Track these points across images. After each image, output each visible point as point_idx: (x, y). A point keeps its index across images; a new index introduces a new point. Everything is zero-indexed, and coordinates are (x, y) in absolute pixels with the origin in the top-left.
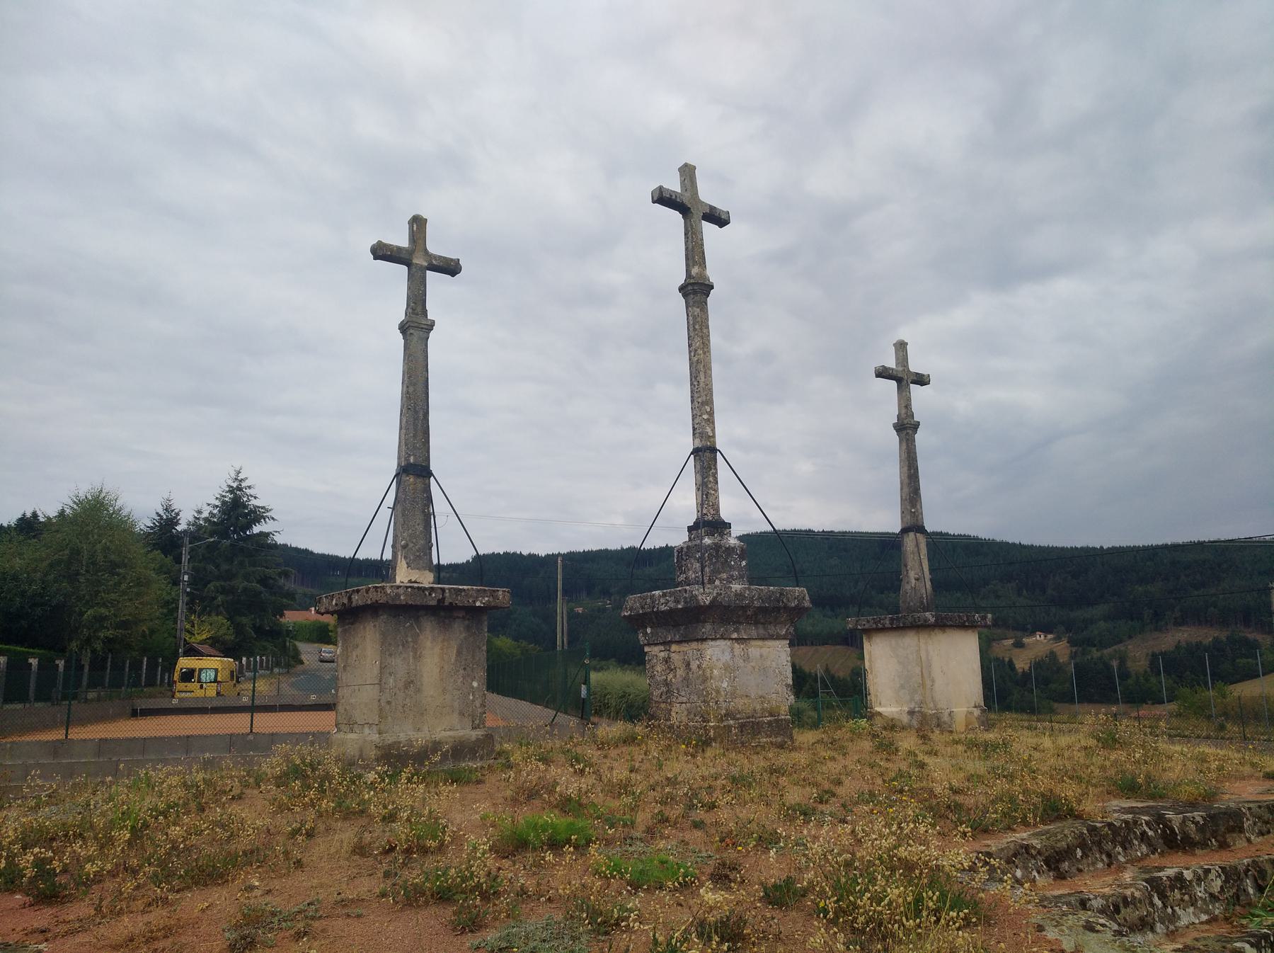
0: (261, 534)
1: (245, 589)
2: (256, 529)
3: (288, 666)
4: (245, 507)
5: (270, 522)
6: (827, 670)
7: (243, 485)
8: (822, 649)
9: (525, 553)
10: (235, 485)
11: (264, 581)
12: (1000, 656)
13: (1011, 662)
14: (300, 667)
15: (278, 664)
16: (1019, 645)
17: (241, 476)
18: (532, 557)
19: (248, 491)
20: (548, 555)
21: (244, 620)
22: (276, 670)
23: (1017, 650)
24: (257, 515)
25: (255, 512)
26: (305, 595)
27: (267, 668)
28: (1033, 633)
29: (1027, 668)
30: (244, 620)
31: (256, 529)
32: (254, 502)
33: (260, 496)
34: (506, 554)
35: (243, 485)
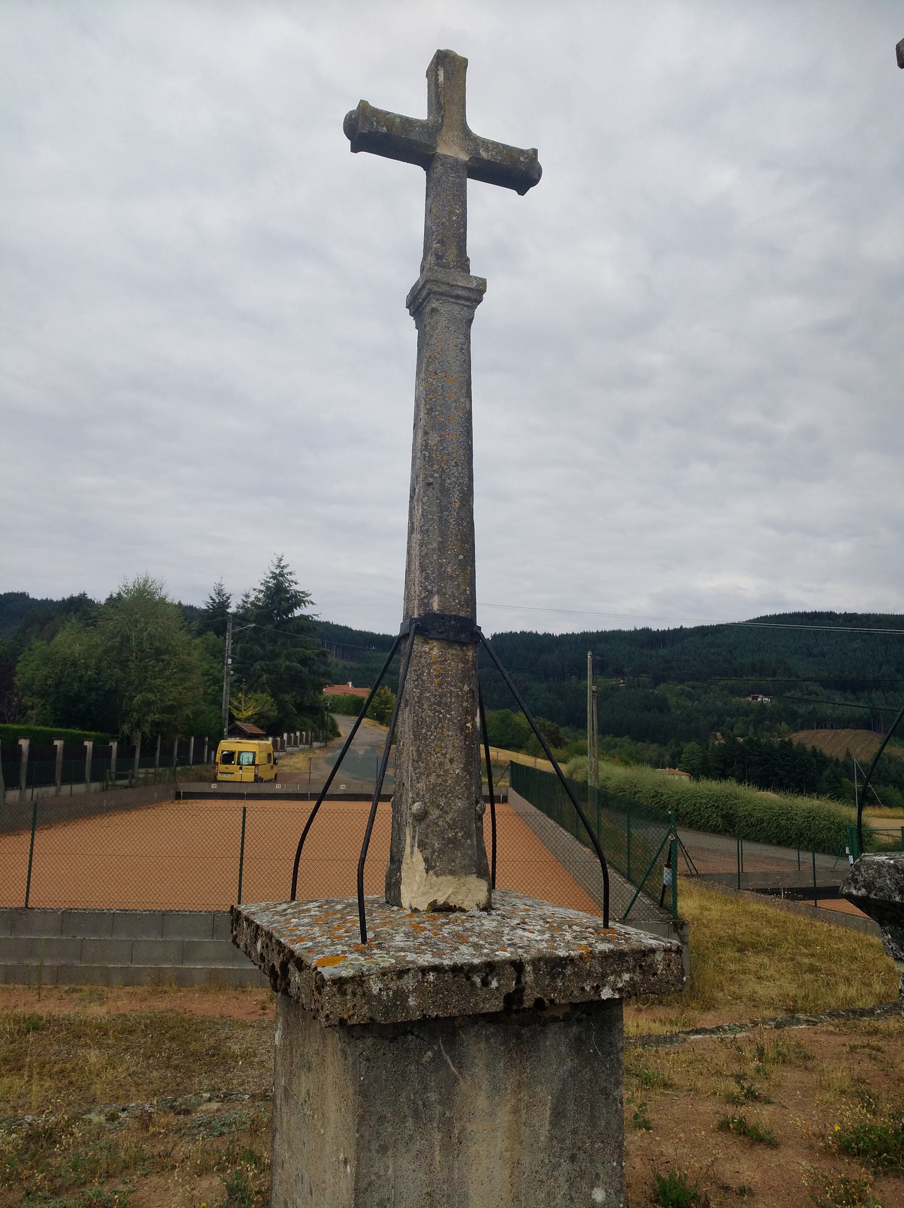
0: (302, 617)
1: (288, 668)
2: (297, 612)
3: (327, 739)
4: (287, 592)
5: (309, 606)
6: (848, 754)
7: (285, 571)
8: (843, 732)
9: (541, 633)
10: (277, 571)
11: (304, 661)
15: (317, 739)
17: (283, 564)
18: (547, 636)
19: (289, 577)
20: (562, 635)
21: (287, 697)
22: (315, 744)
24: (297, 600)
25: (296, 596)
26: (345, 667)
27: (307, 743)
30: (287, 697)
31: (297, 612)
32: (294, 587)
33: (300, 583)
34: (523, 633)
35: (285, 571)
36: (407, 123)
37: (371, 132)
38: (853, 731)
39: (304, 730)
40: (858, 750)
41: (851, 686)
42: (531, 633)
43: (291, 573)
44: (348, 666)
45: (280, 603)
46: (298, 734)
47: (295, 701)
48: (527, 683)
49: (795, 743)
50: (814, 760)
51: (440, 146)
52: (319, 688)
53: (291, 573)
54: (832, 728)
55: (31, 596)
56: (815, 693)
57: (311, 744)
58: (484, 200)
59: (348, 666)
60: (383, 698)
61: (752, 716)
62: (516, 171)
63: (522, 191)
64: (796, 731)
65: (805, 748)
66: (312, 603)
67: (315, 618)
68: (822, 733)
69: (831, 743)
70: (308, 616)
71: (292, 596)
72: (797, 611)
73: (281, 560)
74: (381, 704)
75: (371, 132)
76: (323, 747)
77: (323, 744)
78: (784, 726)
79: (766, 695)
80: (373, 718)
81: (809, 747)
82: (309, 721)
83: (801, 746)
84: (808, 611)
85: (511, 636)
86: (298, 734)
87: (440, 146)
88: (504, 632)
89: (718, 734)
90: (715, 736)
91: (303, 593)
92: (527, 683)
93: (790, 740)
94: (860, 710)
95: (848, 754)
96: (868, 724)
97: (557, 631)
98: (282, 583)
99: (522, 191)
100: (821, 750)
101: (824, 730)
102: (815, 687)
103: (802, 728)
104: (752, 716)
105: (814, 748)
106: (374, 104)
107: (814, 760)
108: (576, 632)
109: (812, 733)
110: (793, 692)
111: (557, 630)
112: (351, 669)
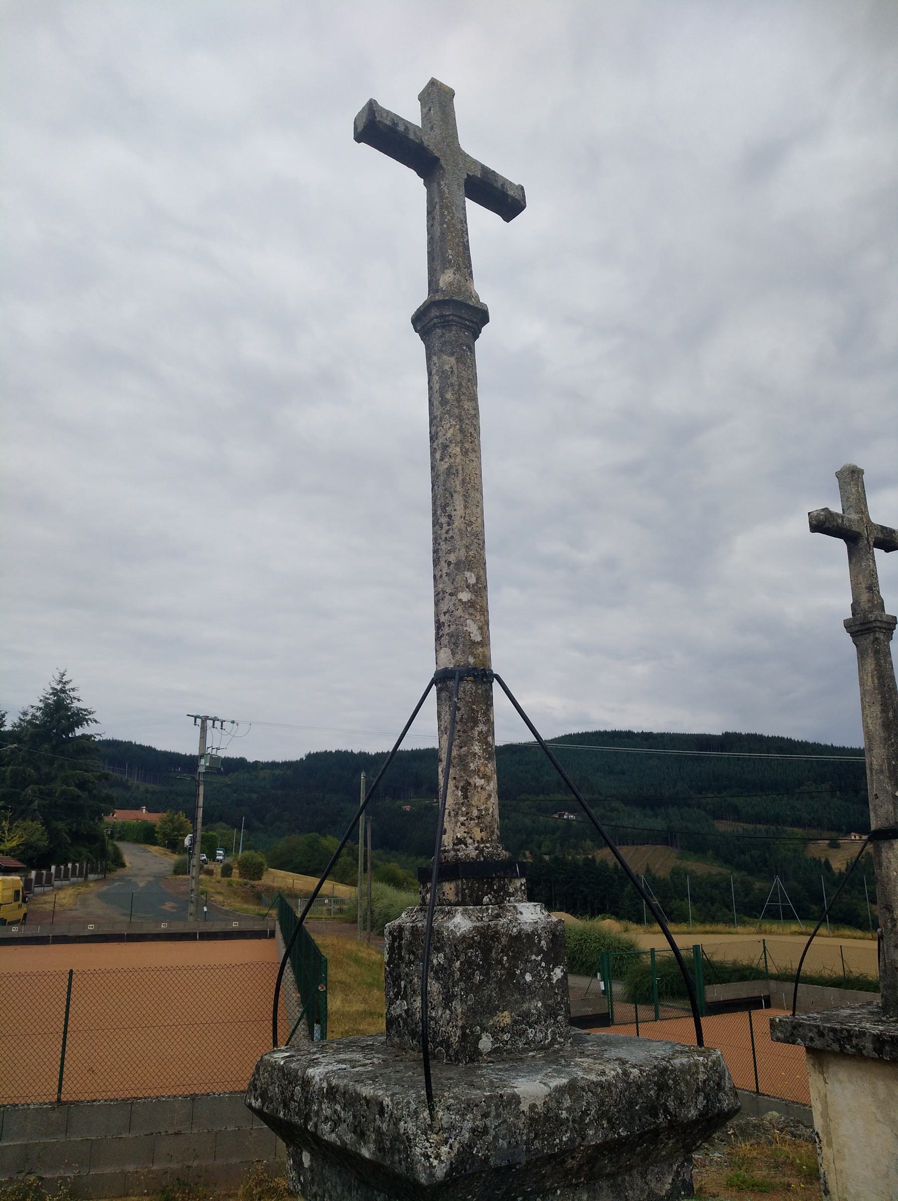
0: (84, 736)
1: (64, 792)
2: (79, 732)
3: (106, 870)
4: (69, 709)
6: (648, 870)
8: (644, 848)
9: (356, 751)
10: (59, 687)
11: (82, 785)
12: (816, 856)
13: (827, 863)
14: (120, 872)
15: (93, 870)
16: (834, 845)
17: (65, 679)
18: (363, 755)
19: (72, 694)
20: (378, 754)
21: (60, 825)
22: (91, 877)
23: (832, 852)
24: (80, 718)
25: (78, 714)
26: (147, 791)
27: (80, 875)
28: (848, 833)
29: (843, 868)
30: (60, 825)
31: (79, 732)
32: (76, 704)
33: (84, 698)
34: (338, 752)
35: (67, 687)
38: (653, 847)
39: (77, 861)
40: (657, 866)
41: (650, 803)
42: (346, 752)
43: (73, 690)
44: (151, 789)
45: (59, 721)
46: (70, 865)
47: (70, 830)
49: (598, 860)
52: (98, 814)
54: (634, 844)
57: (86, 877)
59: (151, 789)
60: (176, 824)
65: (607, 865)
66: (96, 721)
70: (92, 736)
71: (74, 714)
72: (598, 730)
74: (174, 830)
77: (101, 876)
78: (589, 843)
79: (571, 813)
80: (164, 846)
84: (609, 729)
85: (326, 755)
86: (70, 865)
88: (319, 751)
89: (527, 853)
90: (524, 855)
91: (85, 710)
93: (593, 857)
94: (658, 824)
96: (666, 838)
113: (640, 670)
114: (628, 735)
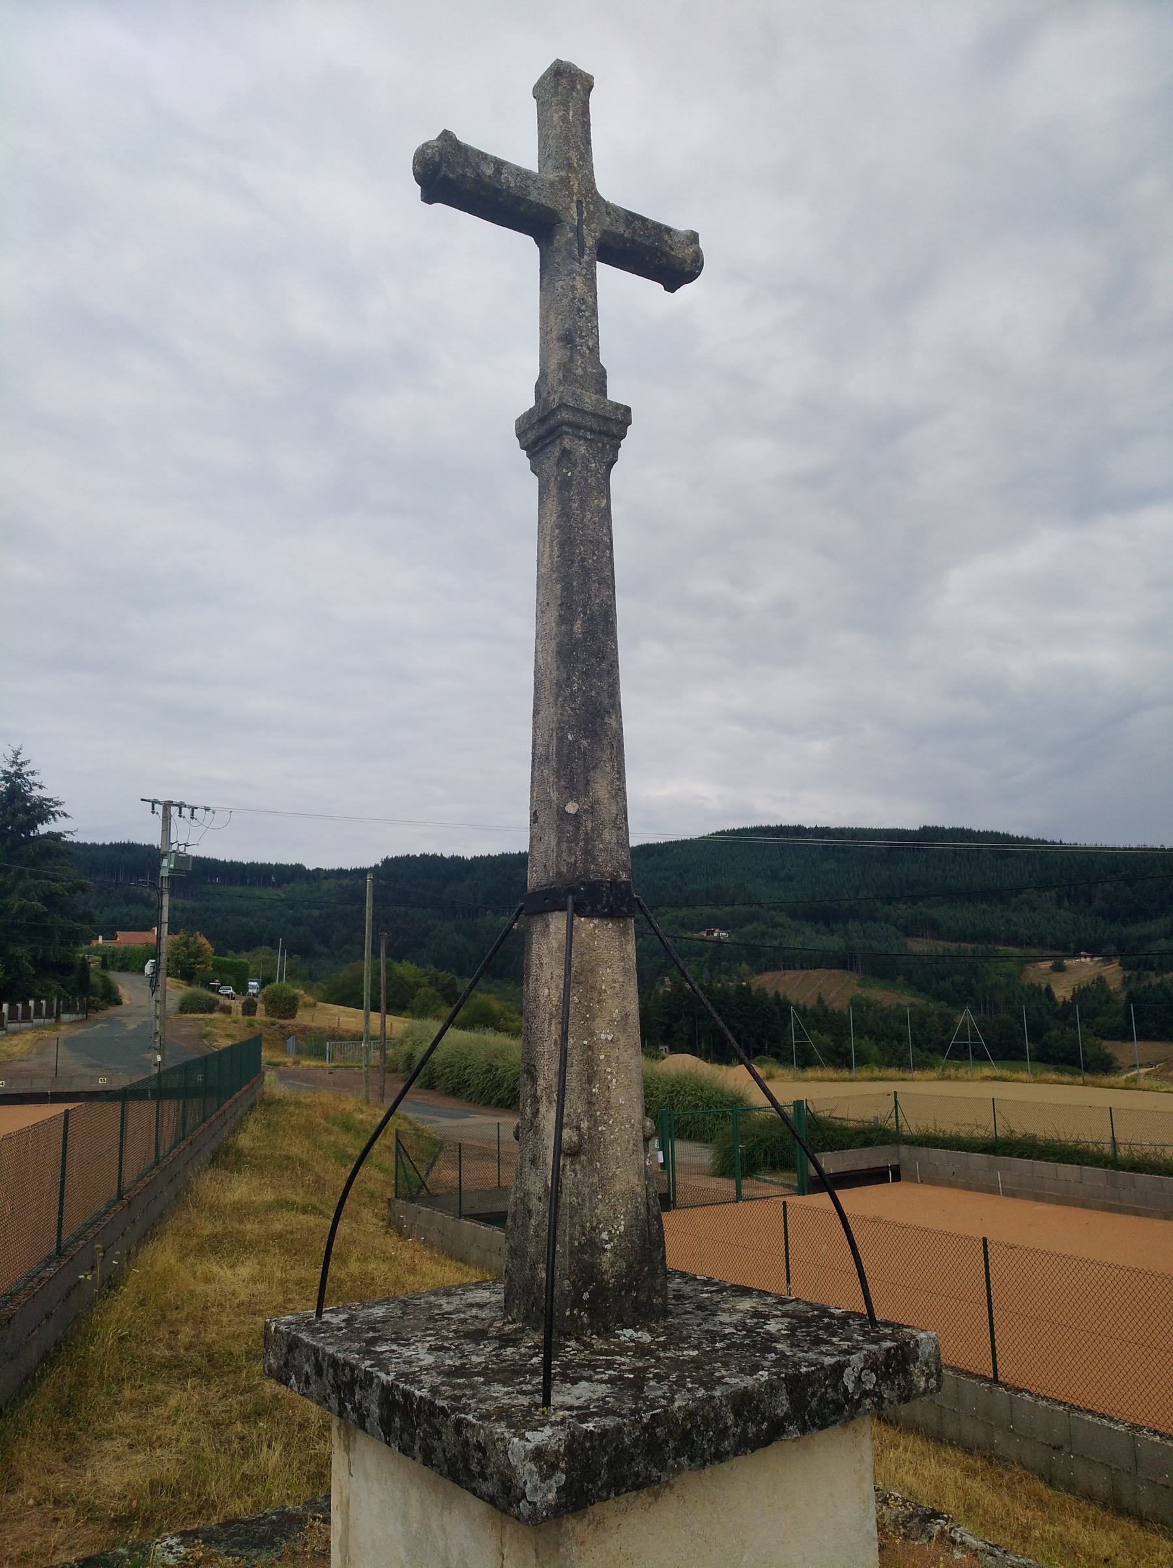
0: (50, 835)
1: (22, 910)
2: (43, 829)
3: (89, 1008)
4: (28, 799)
5: (61, 820)
6: (820, 1001)
7: (24, 769)
8: (815, 973)
9: (447, 855)
10: (12, 770)
11: (49, 899)
12: (1036, 981)
13: (1049, 990)
14: (112, 1010)
15: (68, 1009)
16: (1059, 968)
17: (21, 759)
18: (456, 861)
19: (31, 778)
20: (475, 858)
21: (19, 951)
22: (65, 1017)
23: (1055, 975)
24: (42, 811)
25: (41, 806)
27: (49, 1014)
28: (1076, 954)
29: (1068, 996)
30: (19, 951)
31: (43, 829)
32: (36, 793)
33: (48, 784)
34: (423, 856)
35: (24, 769)
36: (518, 172)
37: (452, 176)
38: (827, 972)
39: (43, 998)
40: (832, 995)
41: (823, 915)
42: (434, 856)
43: (33, 773)
44: (180, 905)
45: (14, 815)
46: (31, 1003)
47: (34, 957)
48: (429, 922)
49: (754, 988)
50: (777, 1009)
51: (556, 211)
52: (76, 938)
53: (33, 773)
54: (802, 968)
55: (947, 827)
56: (781, 925)
57: (58, 1017)
58: (618, 290)
59: (180, 905)
60: (192, 949)
61: (706, 956)
62: (666, 259)
63: (671, 287)
64: (759, 972)
65: (766, 995)
66: (65, 815)
67: (69, 838)
68: (790, 975)
69: (798, 987)
70: (61, 834)
71: (34, 805)
72: (759, 825)
73: (19, 753)
74: (189, 955)
75: (452, 176)
76: (80, 1021)
77: (80, 1016)
78: (745, 967)
79: (722, 929)
80: (176, 977)
81: (771, 995)
82: (55, 985)
83: (761, 990)
84: (773, 825)
85: (408, 860)
86: (31, 1003)
87: (556, 211)
88: (399, 855)
89: (667, 979)
90: (663, 982)
91: (50, 800)
92: (429, 922)
93: (748, 984)
94: (834, 943)
95: (820, 1001)
96: (844, 962)
97: (468, 854)
98: (20, 787)
99: (671, 287)
100: (785, 996)
101: (792, 972)
102: (781, 918)
103: (767, 969)
104: (706, 956)
105: (777, 995)
106: (463, 137)
107: (777, 1009)
108: (492, 854)
109: (778, 974)
110: (755, 924)
111: (468, 853)
112: (184, 910)
113: (818, 747)
114: (799, 831)
